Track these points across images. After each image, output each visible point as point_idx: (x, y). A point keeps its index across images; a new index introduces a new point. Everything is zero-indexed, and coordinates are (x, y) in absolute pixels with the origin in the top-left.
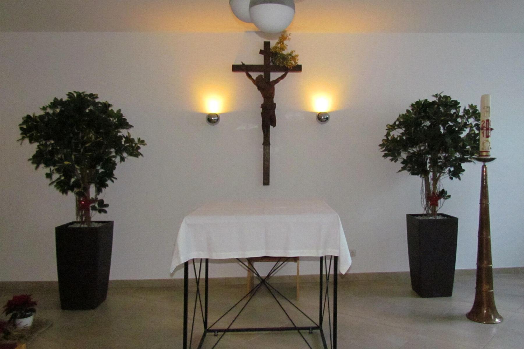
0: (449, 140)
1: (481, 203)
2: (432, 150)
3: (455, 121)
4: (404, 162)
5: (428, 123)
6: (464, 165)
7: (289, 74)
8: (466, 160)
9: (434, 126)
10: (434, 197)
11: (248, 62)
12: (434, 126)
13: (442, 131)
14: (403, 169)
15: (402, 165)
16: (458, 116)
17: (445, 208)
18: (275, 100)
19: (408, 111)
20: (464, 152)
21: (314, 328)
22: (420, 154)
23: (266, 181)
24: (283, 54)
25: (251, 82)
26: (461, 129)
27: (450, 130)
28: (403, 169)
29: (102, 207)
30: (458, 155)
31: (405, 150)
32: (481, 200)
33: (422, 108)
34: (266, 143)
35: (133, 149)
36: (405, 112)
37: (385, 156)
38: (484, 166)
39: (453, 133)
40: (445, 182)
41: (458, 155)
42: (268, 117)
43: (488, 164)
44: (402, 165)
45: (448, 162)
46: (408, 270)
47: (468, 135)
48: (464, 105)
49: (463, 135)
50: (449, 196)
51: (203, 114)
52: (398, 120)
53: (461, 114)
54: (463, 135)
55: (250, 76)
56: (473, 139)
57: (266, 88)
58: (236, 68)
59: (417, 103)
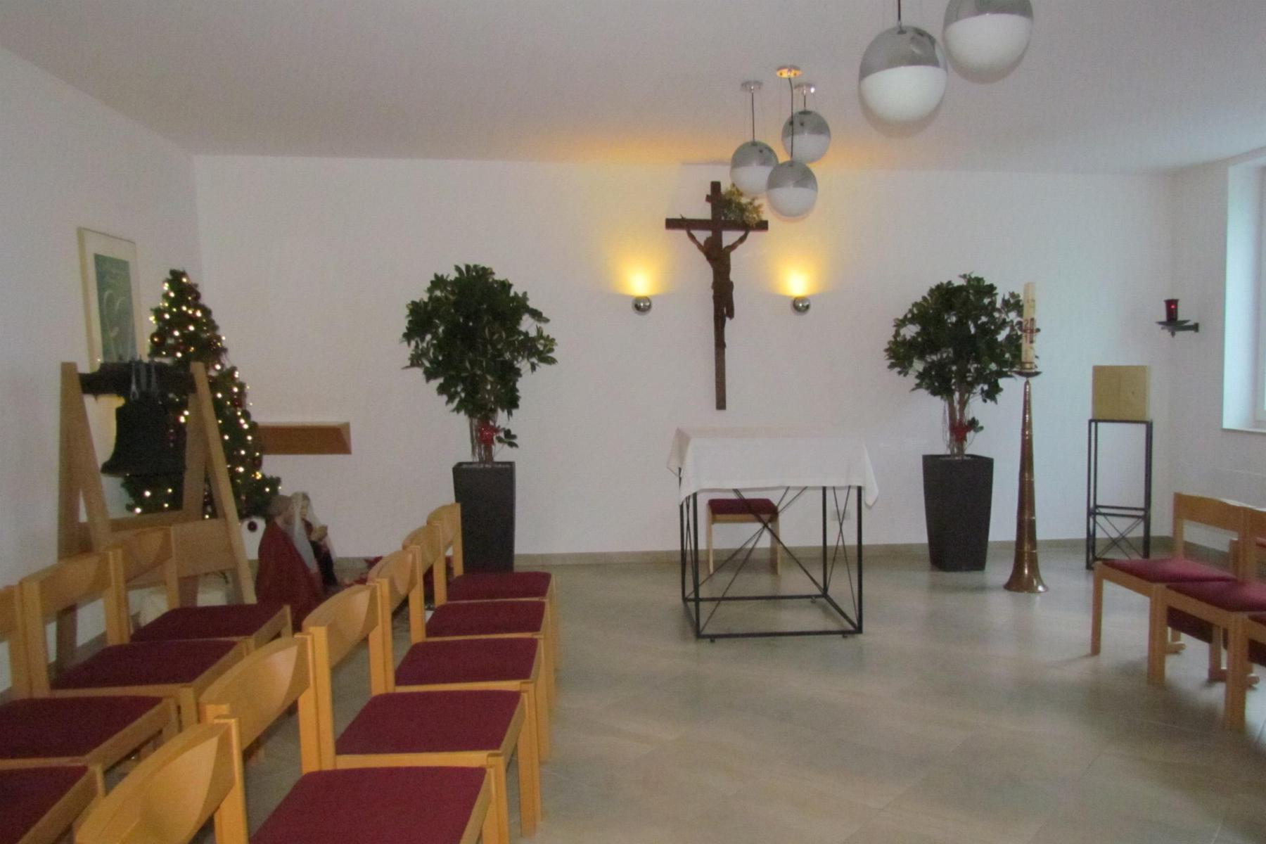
0: (982, 345)
1: (1023, 435)
2: (960, 358)
3: (990, 315)
4: (921, 376)
5: (954, 319)
6: (1002, 382)
7: (752, 234)
8: (1005, 375)
9: (961, 323)
10: (961, 429)
11: (690, 215)
12: (961, 323)
13: (973, 331)
14: (918, 386)
15: (917, 381)
16: (994, 309)
17: (975, 445)
18: (732, 277)
19: (924, 298)
20: (1002, 363)
21: (817, 596)
22: (941, 367)
23: (721, 404)
24: (739, 204)
25: (694, 247)
26: (997, 331)
27: (982, 329)
28: (918, 386)
29: (509, 439)
30: (993, 366)
31: (922, 357)
32: (1024, 430)
33: (945, 296)
34: (720, 344)
35: (540, 350)
36: (919, 299)
37: (892, 366)
38: (1027, 383)
39: (987, 332)
40: (977, 407)
41: (993, 366)
42: (724, 302)
43: (1032, 380)
44: (917, 381)
45: (981, 377)
46: (924, 539)
47: (1009, 337)
48: (1001, 294)
49: (1002, 336)
50: (982, 428)
51: (628, 297)
52: (911, 311)
53: (998, 305)
54: (1002, 336)
55: (692, 237)
56: (1014, 343)
57: (718, 257)
58: (672, 224)
59: (939, 287)
